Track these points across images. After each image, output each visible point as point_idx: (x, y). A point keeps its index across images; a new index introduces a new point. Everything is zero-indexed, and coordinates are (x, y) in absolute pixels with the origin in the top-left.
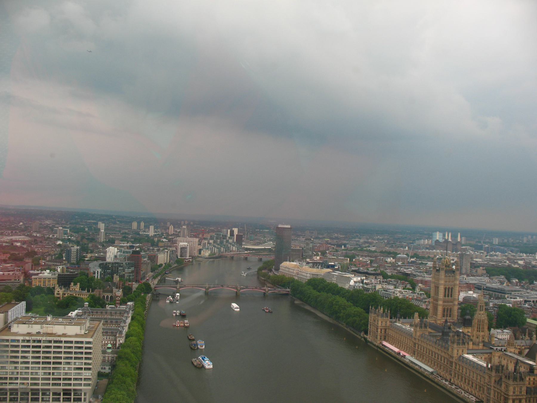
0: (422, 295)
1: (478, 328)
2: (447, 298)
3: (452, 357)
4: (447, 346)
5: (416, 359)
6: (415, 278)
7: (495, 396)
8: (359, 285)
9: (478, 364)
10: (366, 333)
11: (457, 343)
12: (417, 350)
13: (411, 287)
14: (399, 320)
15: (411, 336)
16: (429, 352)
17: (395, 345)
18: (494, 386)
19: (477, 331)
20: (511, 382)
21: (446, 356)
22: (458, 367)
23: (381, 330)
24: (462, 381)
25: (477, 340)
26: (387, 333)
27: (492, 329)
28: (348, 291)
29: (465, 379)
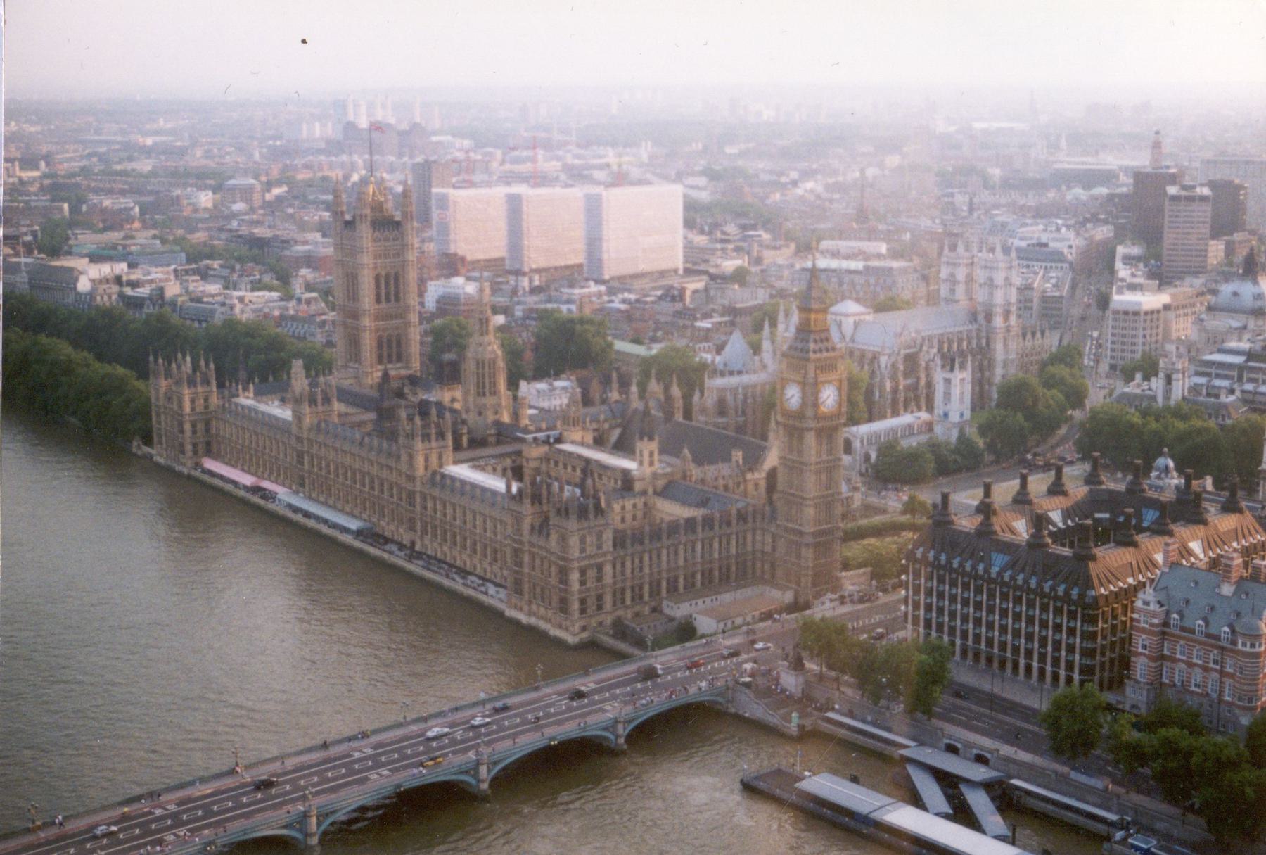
0: (313, 303)
1: (478, 387)
2: (384, 305)
3: (411, 478)
4: (394, 447)
5: (310, 498)
6: (287, 253)
7: (534, 568)
8: (109, 291)
9: (484, 490)
10: (148, 440)
12: (310, 472)
13: (275, 282)
14: (246, 389)
15: (289, 432)
16: (346, 472)
17: (242, 465)
18: (532, 540)
19: (478, 394)
20: (572, 524)
21: (394, 477)
22: (430, 504)
23: (194, 425)
26: (214, 431)
27: (523, 385)
29: (454, 536)
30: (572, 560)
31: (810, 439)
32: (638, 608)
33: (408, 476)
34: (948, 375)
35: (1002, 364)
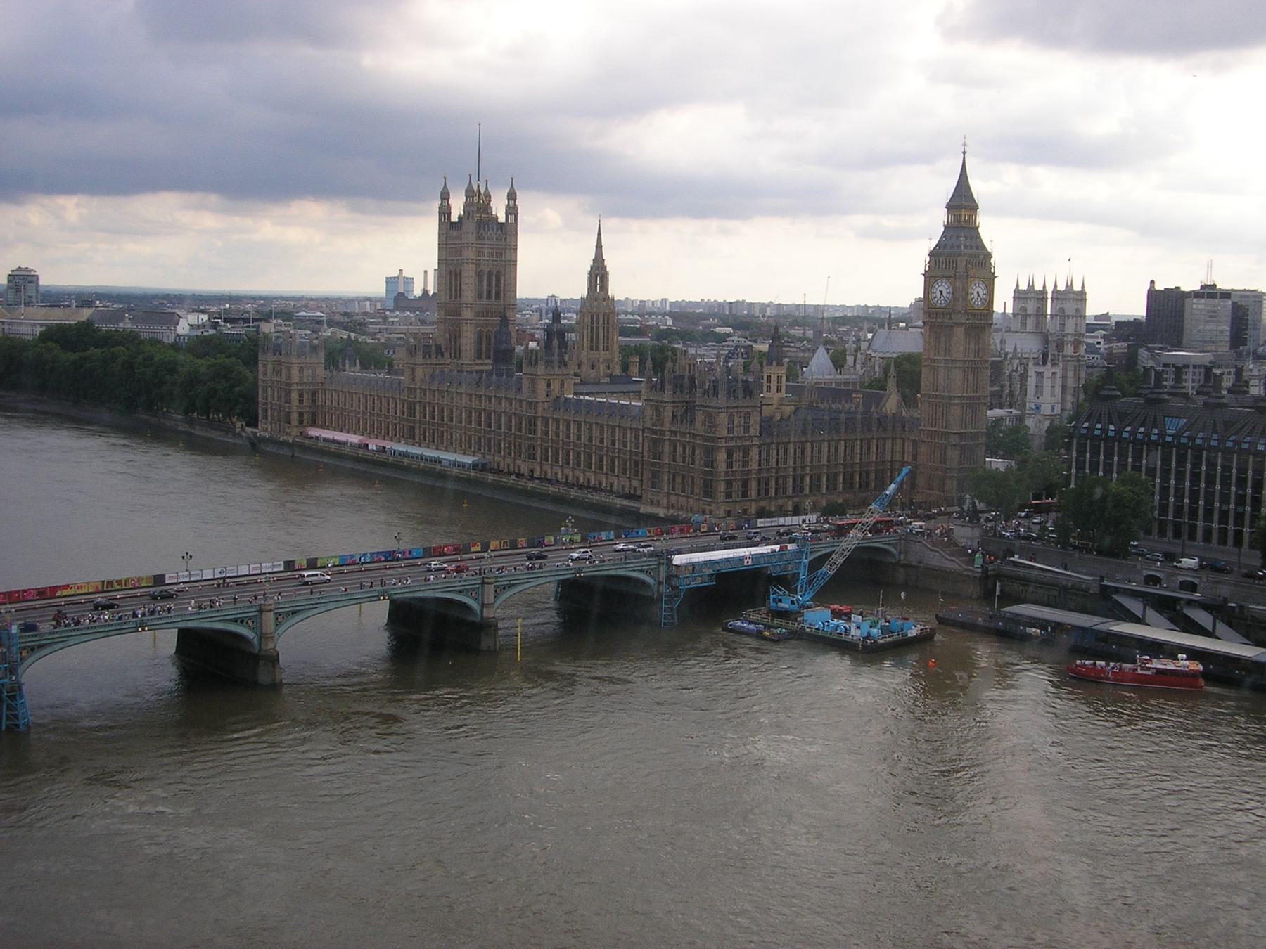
1: (592, 342)
2: (485, 301)
3: (532, 405)
5: (420, 446)
10: (253, 422)
11: (547, 361)
14: (353, 364)
16: (461, 415)
18: (673, 429)
19: (592, 349)
20: (721, 400)
22: (552, 428)
23: (301, 395)
24: (568, 464)
25: (593, 374)
28: (175, 346)
30: (720, 438)
31: (959, 331)
32: (780, 502)
33: (529, 403)
34: (1041, 369)
35: (1072, 391)
